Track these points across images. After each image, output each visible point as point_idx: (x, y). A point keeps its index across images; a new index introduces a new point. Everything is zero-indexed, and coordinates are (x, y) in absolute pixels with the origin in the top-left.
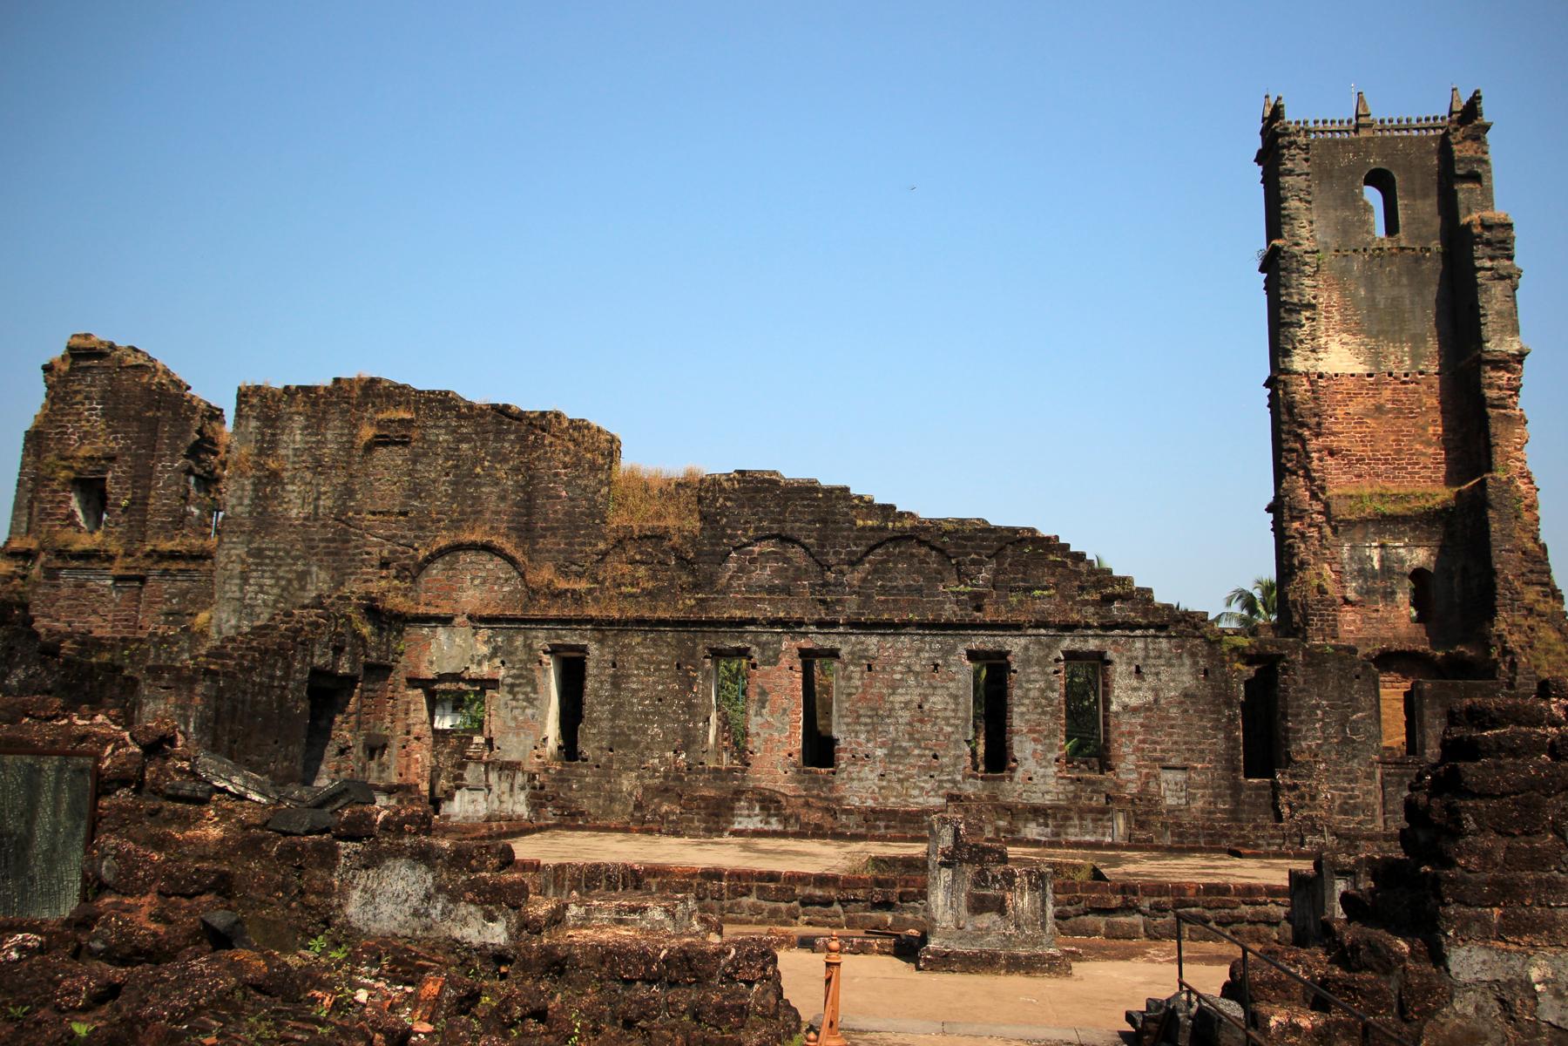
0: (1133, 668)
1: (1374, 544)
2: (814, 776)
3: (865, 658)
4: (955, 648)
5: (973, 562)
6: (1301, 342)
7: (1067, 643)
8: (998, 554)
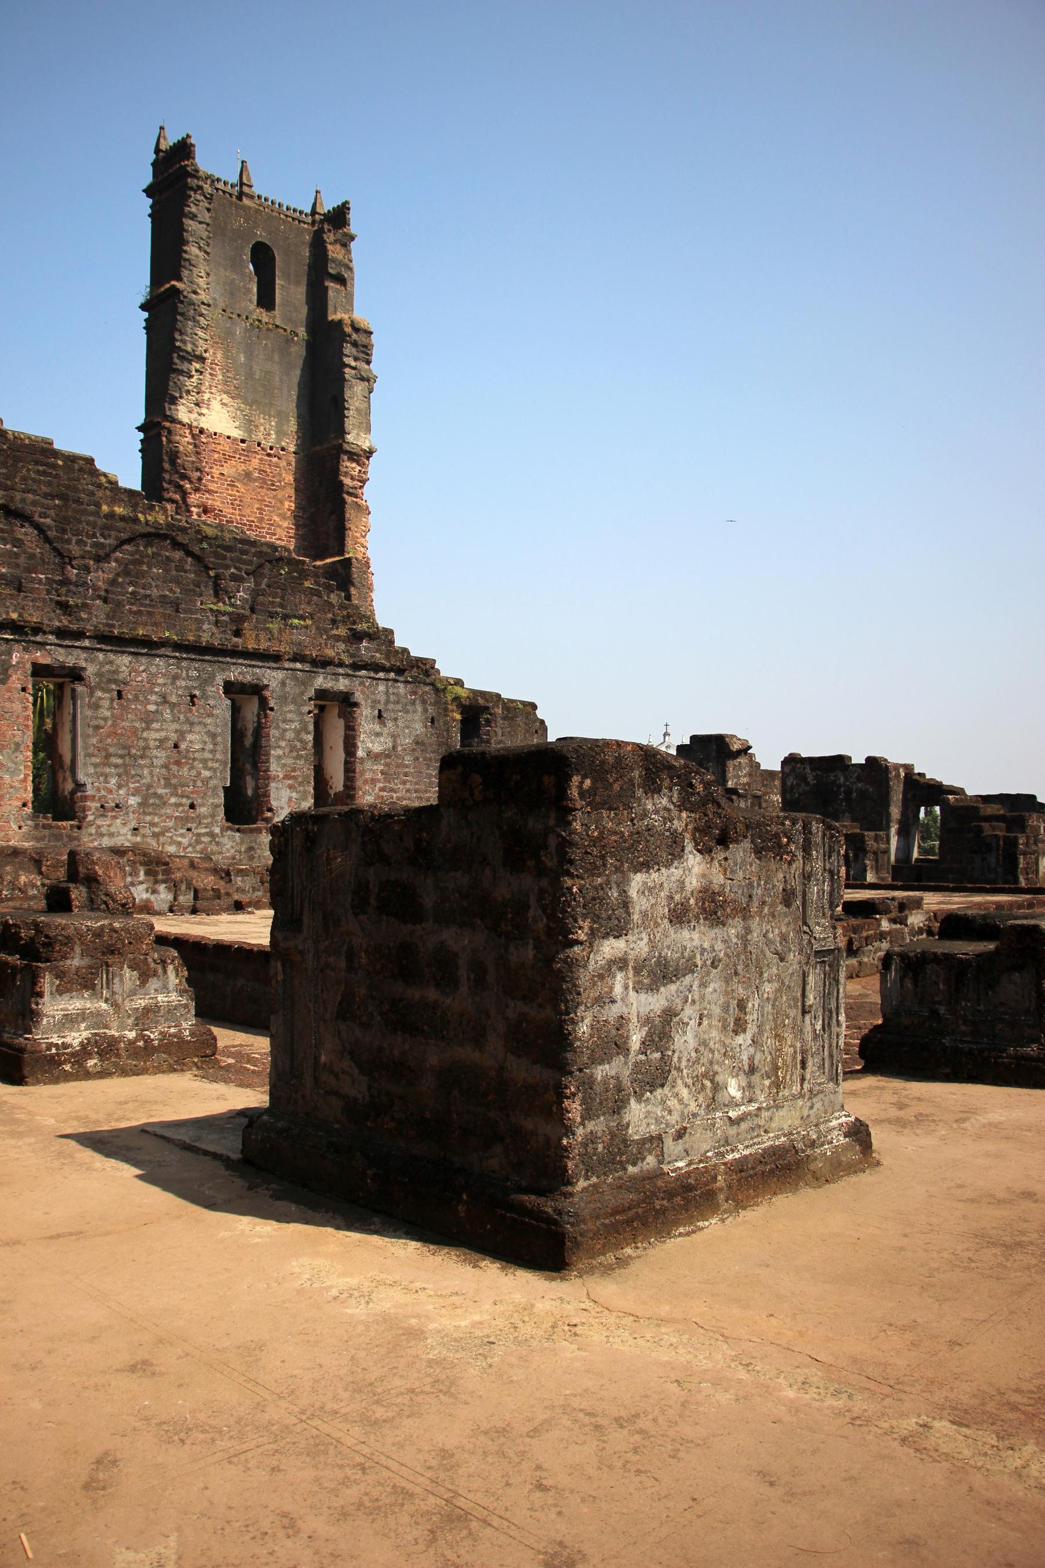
0: (377, 712)
2: (56, 831)
3: (115, 681)
4: (213, 677)
5: (235, 578)
6: (188, 392)
7: (321, 681)
8: (255, 573)
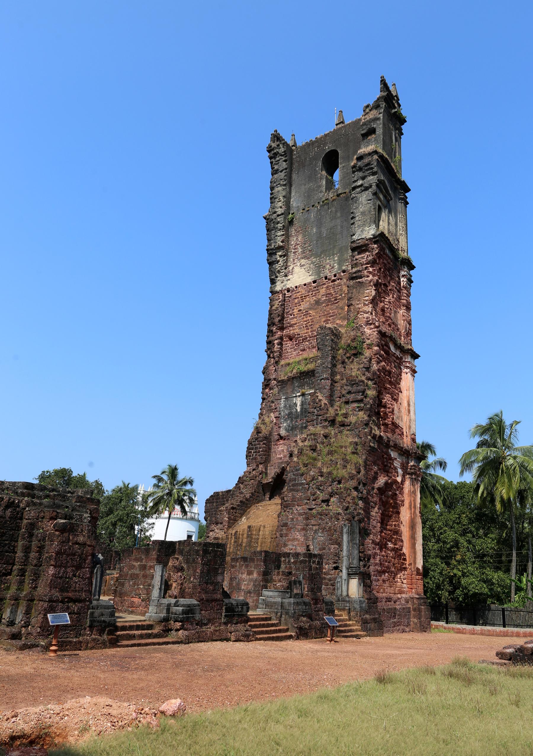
1: (298, 394)
6: (279, 272)
